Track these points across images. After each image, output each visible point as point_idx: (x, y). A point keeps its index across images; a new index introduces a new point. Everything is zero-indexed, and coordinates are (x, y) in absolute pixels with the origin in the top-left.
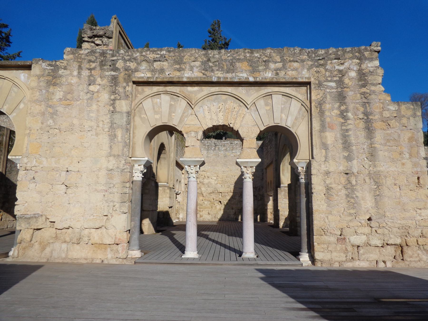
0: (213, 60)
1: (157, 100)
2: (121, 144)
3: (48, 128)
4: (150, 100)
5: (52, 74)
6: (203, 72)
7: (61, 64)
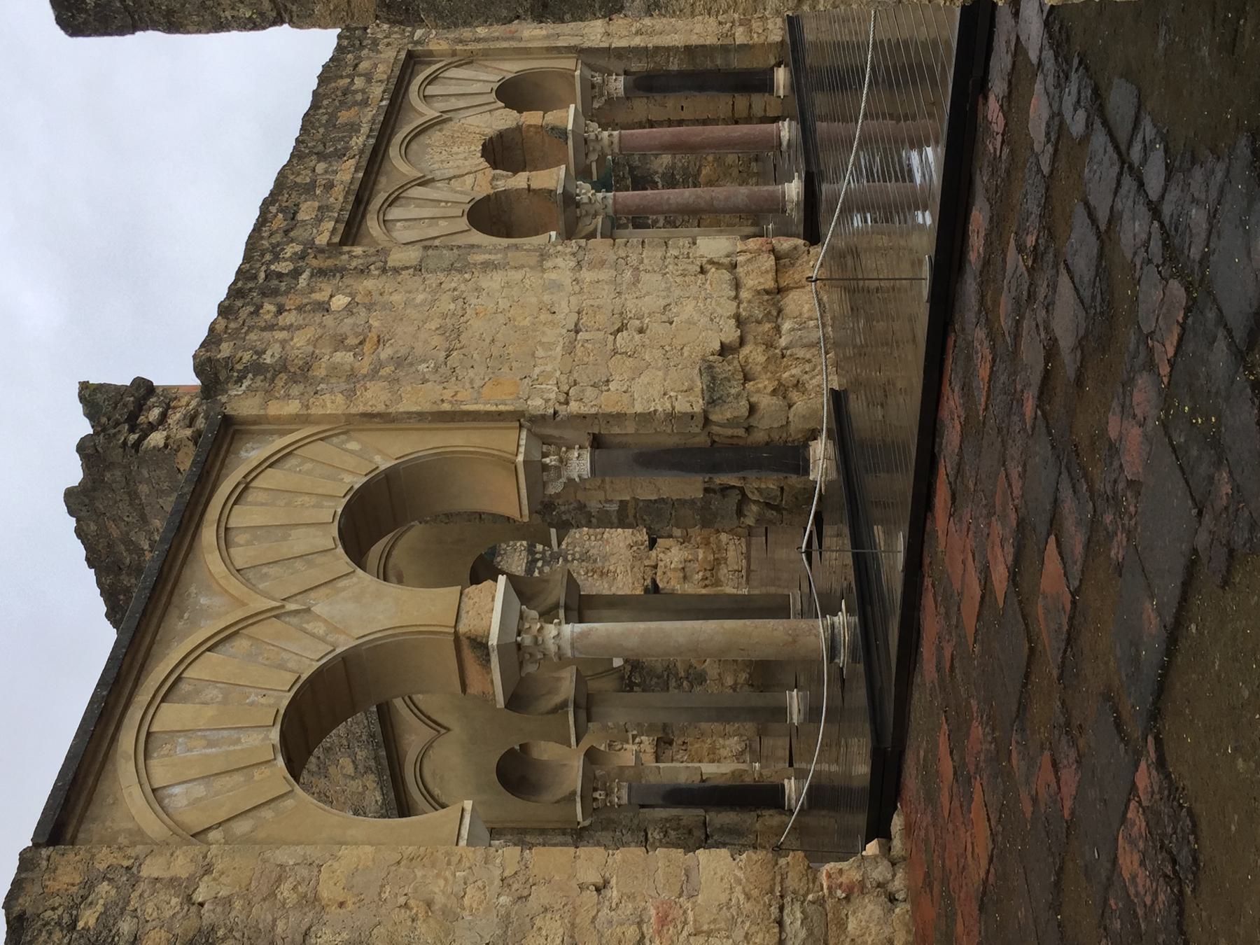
5: (269, 375)
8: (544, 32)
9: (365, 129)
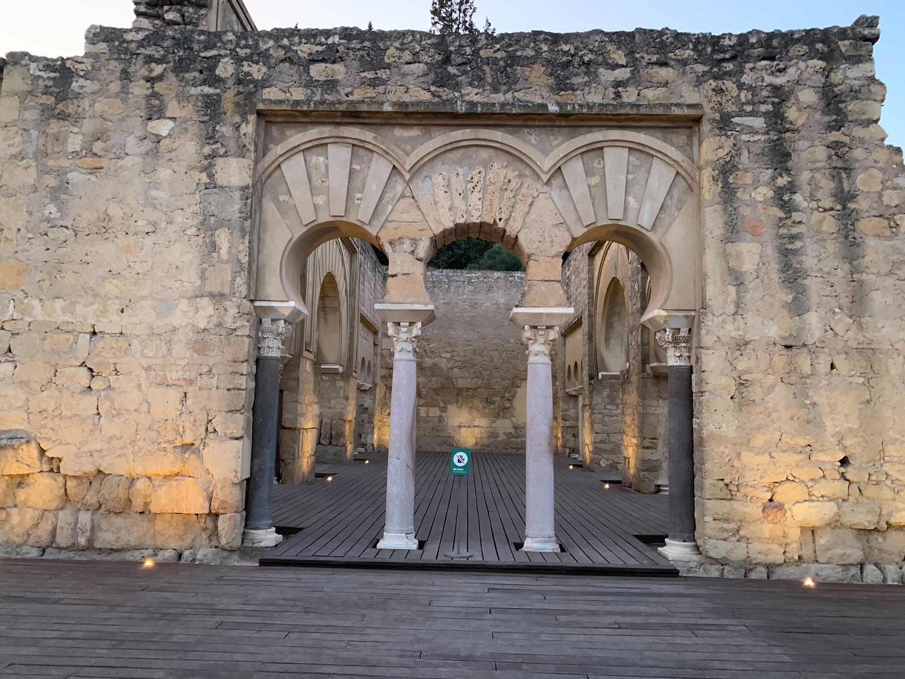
0: (459, 60)
1: (317, 159)
2: (228, 268)
3: (44, 226)
4: (300, 157)
5: (54, 89)
6: (433, 88)
7: (77, 66)
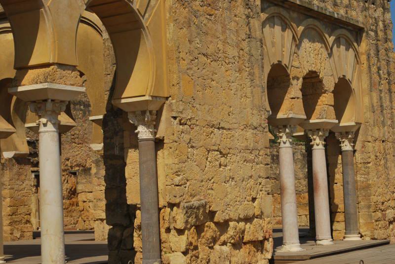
8: (375, 105)
9: (322, 5)
